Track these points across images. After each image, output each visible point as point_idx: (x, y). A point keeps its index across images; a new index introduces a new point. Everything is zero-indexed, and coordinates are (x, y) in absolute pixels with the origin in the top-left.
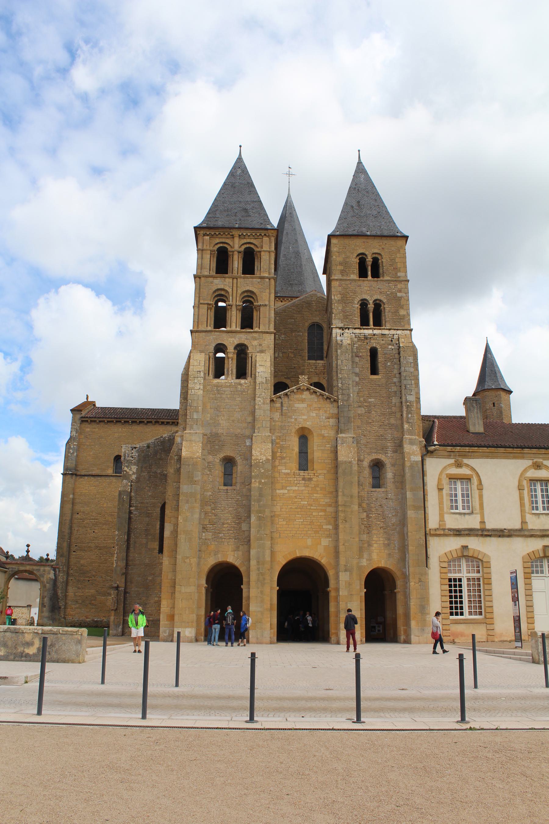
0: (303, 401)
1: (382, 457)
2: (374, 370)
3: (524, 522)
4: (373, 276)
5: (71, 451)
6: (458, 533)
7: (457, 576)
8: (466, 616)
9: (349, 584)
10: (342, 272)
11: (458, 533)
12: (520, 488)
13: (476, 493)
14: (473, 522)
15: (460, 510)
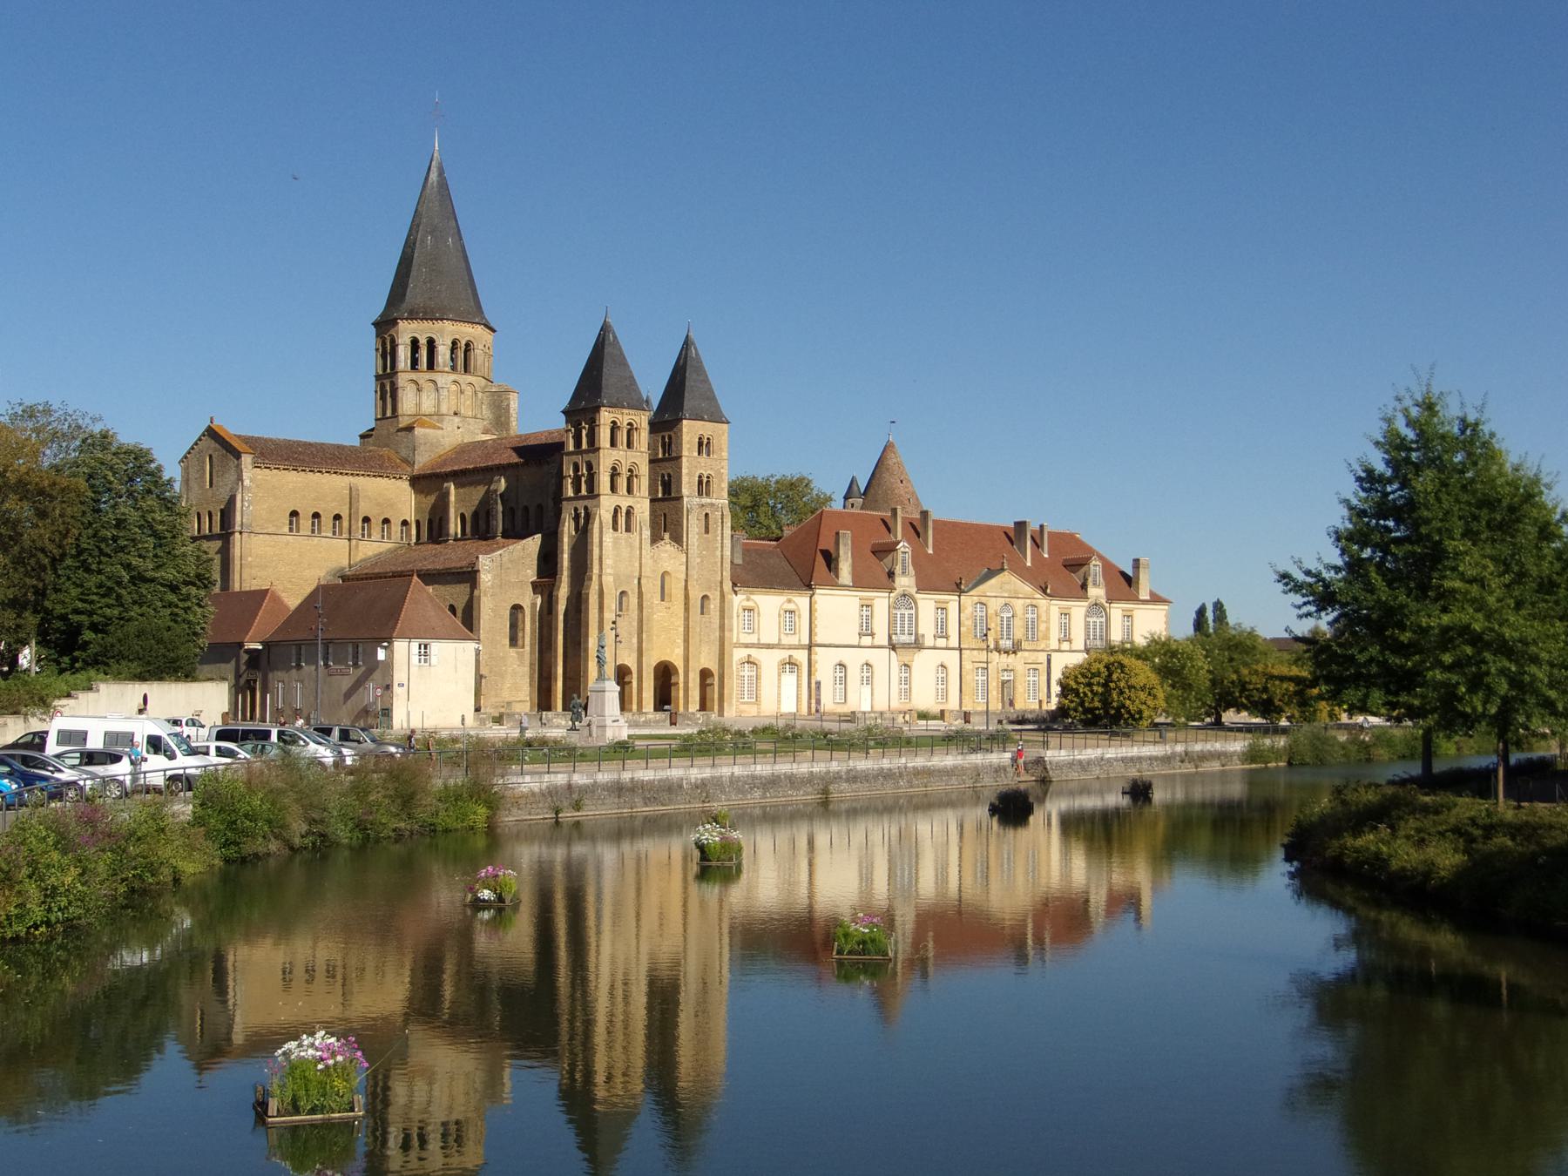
0: (666, 551)
1: (709, 594)
2: (707, 531)
3: (780, 640)
4: (709, 455)
5: (246, 504)
6: (747, 646)
7: (742, 674)
8: (746, 700)
9: (694, 679)
10: (689, 449)
11: (747, 646)
12: (780, 616)
13: (756, 618)
14: (753, 639)
15: (746, 630)
